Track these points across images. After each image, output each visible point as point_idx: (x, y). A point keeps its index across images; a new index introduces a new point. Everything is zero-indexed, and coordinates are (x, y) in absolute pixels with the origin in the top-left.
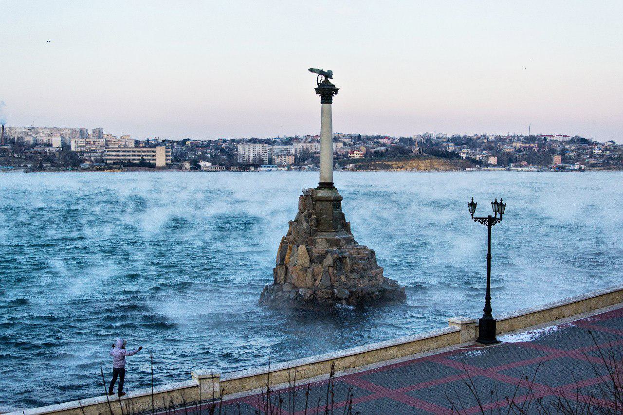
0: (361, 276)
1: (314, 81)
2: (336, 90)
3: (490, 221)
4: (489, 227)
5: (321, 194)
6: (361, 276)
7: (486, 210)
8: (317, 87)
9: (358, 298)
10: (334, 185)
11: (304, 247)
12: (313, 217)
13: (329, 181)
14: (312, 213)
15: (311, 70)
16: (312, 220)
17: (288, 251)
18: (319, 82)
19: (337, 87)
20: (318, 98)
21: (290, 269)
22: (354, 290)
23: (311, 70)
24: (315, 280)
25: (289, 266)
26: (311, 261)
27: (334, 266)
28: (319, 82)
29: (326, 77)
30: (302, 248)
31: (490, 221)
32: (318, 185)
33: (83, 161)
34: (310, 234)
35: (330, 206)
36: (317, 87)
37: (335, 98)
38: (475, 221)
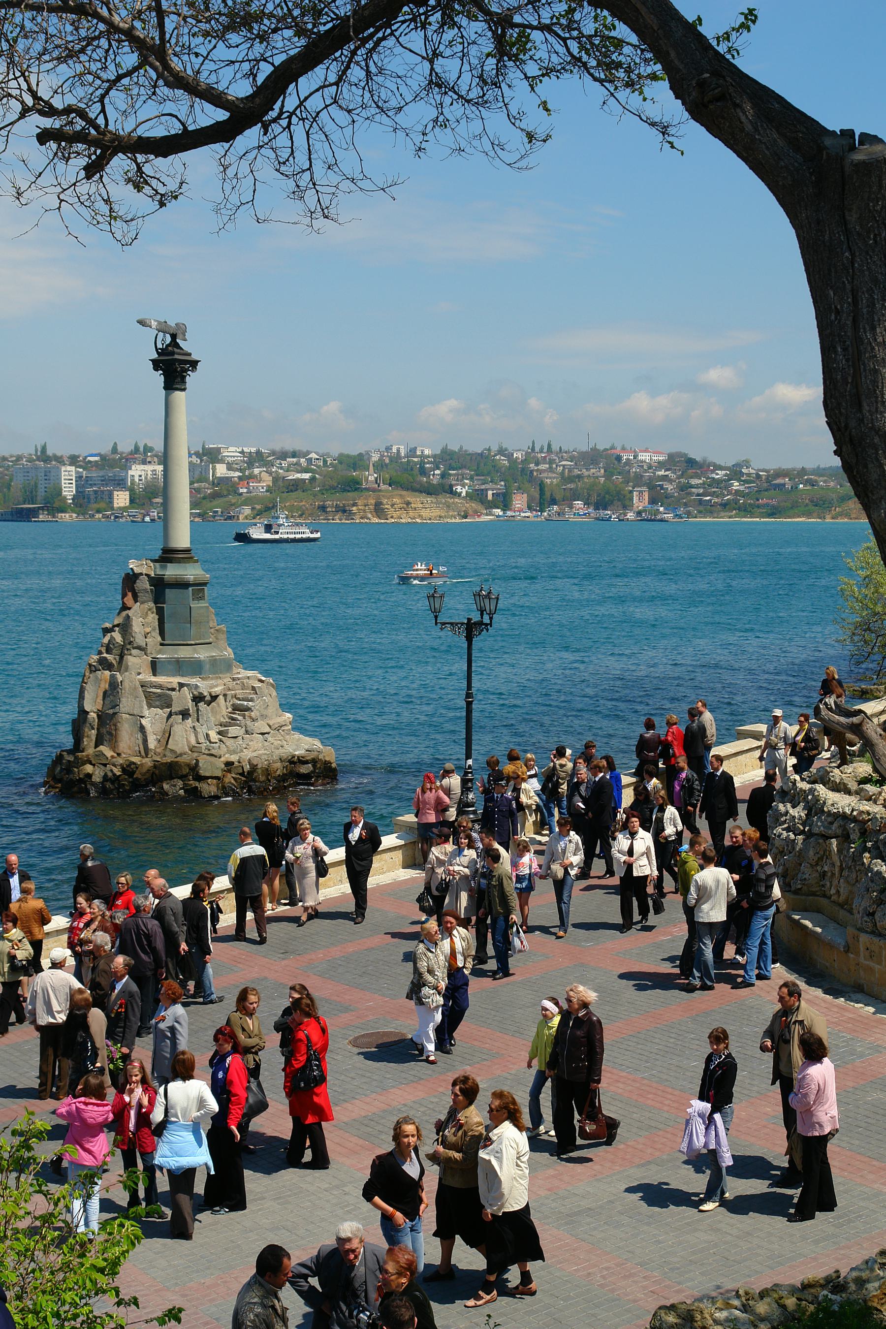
0: (247, 732)
2: (194, 364)
3: (471, 629)
4: (469, 639)
6: (247, 732)
7: (461, 608)
8: (155, 356)
9: (242, 774)
18: (160, 346)
19: (194, 357)
20: (159, 378)
22: (234, 758)
28: (160, 346)
29: (174, 337)
31: (471, 629)
36: (155, 356)
37: (192, 379)
38: (442, 629)
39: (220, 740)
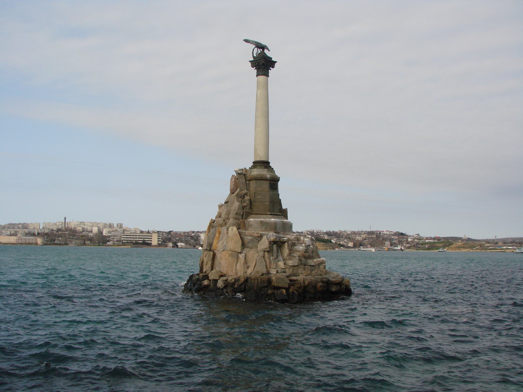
1: (249, 53)
5: (256, 172)
10: (271, 165)
11: (235, 229)
12: (247, 198)
13: (263, 159)
14: (245, 194)
15: (247, 41)
16: (244, 202)
17: (217, 235)
20: (254, 71)
21: (218, 255)
23: (247, 41)
24: (248, 268)
25: (216, 251)
26: (243, 245)
27: (270, 251)
30: (233, 230)
32: (252, 164)
33: (108, 241)
34: (243, 215)
35: (266, 185)
39: (286, 268)
